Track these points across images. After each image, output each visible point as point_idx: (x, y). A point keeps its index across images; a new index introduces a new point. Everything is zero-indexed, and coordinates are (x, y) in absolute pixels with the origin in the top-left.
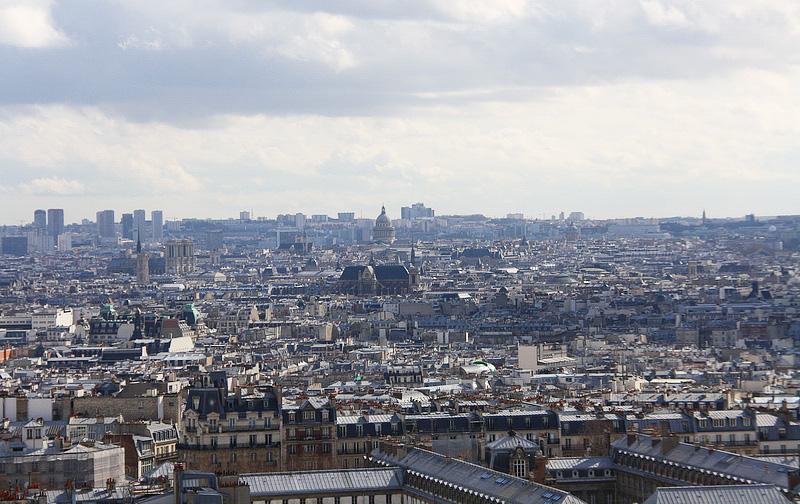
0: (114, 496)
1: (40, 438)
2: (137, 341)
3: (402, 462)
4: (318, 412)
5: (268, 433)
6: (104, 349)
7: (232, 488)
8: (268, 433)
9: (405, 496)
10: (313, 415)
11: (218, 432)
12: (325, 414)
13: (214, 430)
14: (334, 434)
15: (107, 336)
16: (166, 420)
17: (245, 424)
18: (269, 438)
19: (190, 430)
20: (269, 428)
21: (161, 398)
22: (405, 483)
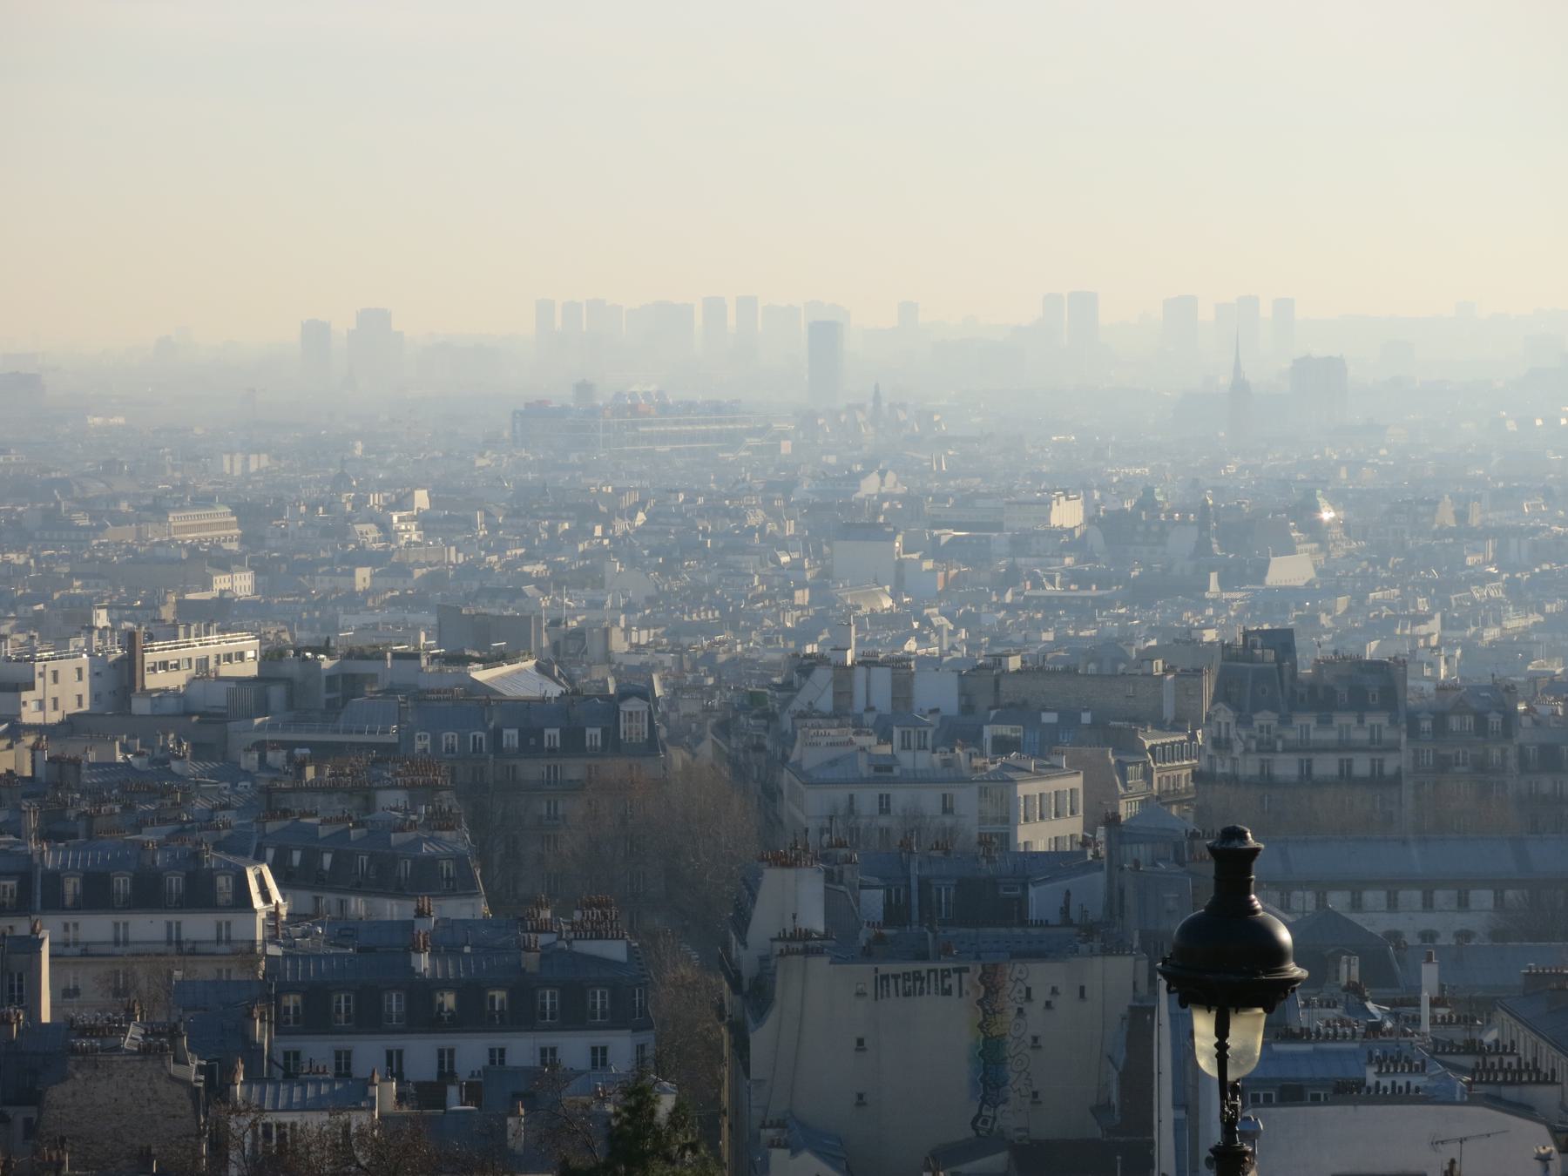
4: (1481, 718)
5: (1378, 756)
11: (1274, 750)
12: (1495, 719)
13: (1266, 747)
14: (1512, 762)
17: (1331, 735)
19: (1220, 744)
20: (1376, 746)
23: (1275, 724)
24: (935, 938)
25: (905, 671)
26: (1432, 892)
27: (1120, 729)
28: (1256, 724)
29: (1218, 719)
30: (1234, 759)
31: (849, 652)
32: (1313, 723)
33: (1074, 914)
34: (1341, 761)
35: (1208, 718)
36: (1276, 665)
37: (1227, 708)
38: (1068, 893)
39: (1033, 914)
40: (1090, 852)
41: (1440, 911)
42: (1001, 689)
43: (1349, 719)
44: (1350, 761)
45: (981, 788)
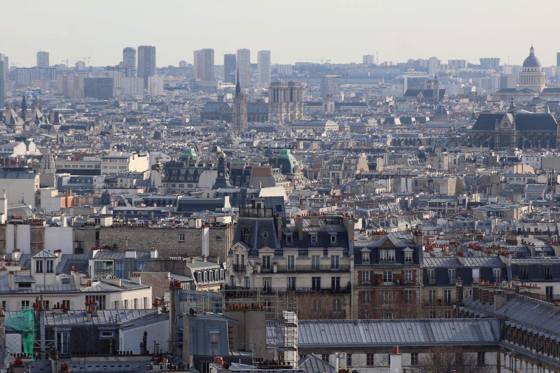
0: (95, 321)
1: (52, 271)
2: (220, 190)
3: (501, 312)
4: (400, 252)
5: (336, 275)
6: (180, 197)
7: (242, 313)
8: (336, 275)
9: (502, 355)
10: (392, 254)
11: (272, 272)
13: (267, 268)
14: (419, 279)
15: (186, 185)
16: (212, 258)
17: (307, 263)
18: (336, 282)
19: (239, 269)
21: (206, 230)
22: (503, 338)
23: (272, 255)
24: (56, 363)
25: (39, 227)
26: (372, 355)
27: (175, 261)
28: (261, 256)
29: (237, 253)
30: (247, 278)
31: (3, 216)
32: (296, 255)
33: (150, 348)
34: (313, 278)
35: (231, 252)
36: (273, 219)
37: (242, 246)
38: (146, 334)
39: (122, 348)
40: (160, 309)
41: (378, 367)
42: (100, 238)
43: (319, 252)
44: (319, 278)
45: (87, 297)
